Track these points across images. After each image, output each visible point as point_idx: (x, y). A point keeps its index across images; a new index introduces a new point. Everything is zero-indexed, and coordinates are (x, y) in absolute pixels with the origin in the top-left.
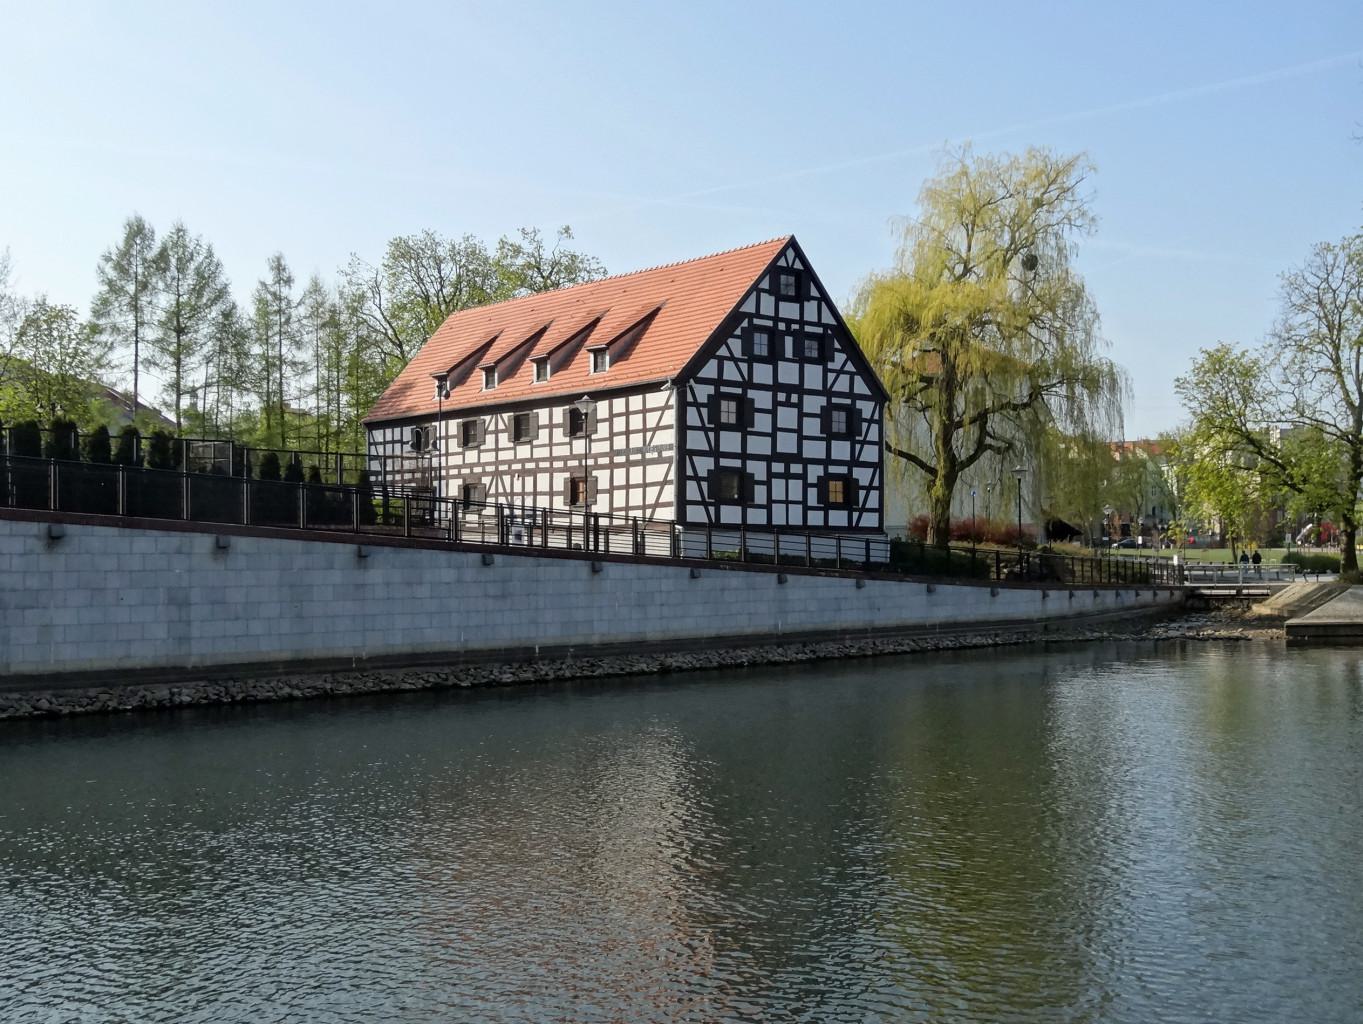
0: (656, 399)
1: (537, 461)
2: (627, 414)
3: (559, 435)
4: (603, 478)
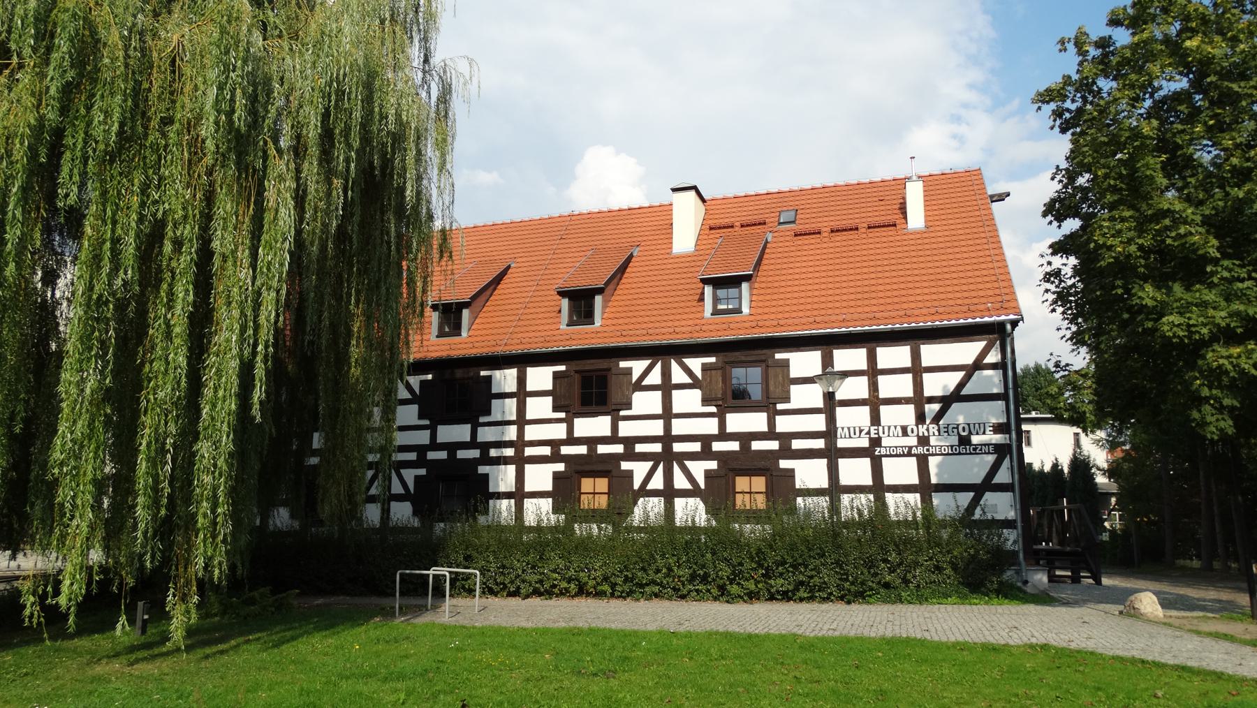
0: (966, 352)
1: (630, 442)
2: (873, 372)
3: (687, 400)
4: (811, 474)
